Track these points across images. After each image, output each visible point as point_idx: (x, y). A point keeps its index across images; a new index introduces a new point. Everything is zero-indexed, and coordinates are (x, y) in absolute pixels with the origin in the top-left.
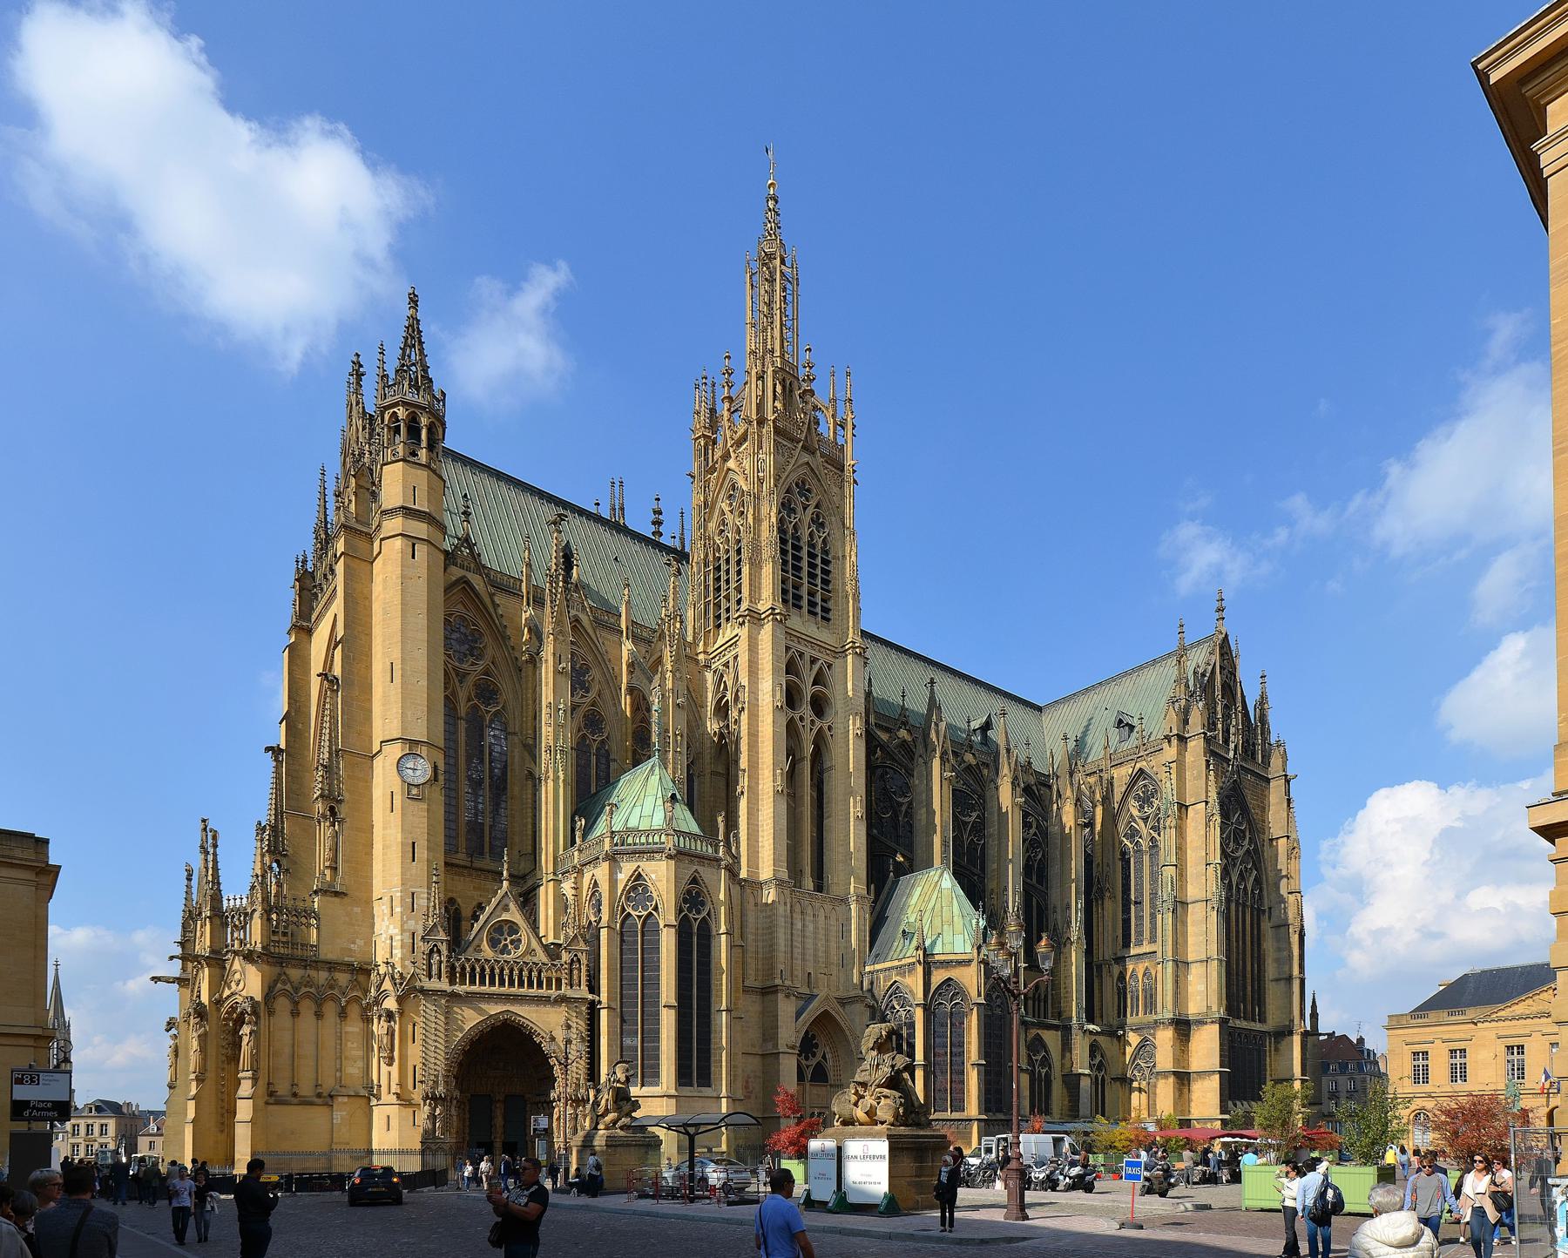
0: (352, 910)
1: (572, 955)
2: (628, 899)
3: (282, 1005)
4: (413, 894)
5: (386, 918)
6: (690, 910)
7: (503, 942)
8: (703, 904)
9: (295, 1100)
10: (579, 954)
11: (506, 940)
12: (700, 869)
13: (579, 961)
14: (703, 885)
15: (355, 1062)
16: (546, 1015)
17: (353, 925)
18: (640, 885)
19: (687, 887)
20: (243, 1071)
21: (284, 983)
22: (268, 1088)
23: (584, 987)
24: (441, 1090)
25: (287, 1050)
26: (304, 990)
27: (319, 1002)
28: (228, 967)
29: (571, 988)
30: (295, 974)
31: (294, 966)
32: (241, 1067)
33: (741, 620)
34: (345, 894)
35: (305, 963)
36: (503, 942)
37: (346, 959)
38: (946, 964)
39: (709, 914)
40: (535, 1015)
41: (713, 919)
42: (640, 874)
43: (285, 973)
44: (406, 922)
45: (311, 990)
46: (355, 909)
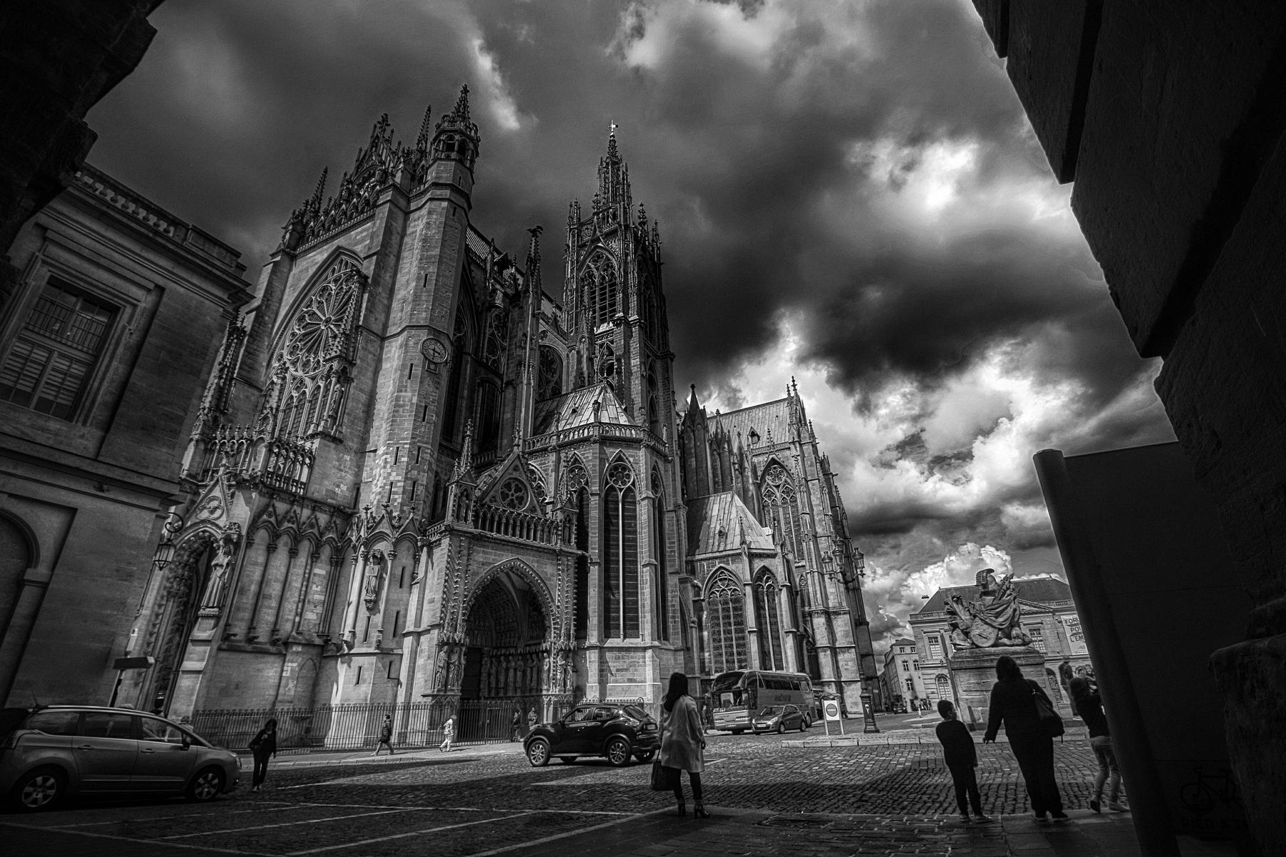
0: (343, 457)
2: (611, 475)
4: (419, 448)
5: (388, 466)
7: (510, 497)
9: (249, 648)
11: (512, 495)
15: (315, 607)
17: (341, 470)
18: (620, 465)
20: (207, 607)
22: (249, 633)
24: (459, 635)
25: (253, 588)
27: (296, 539)
28: (203, 492)
30: (281, 507)
31: (282, 500)
32: (204, 602)
34: (341, 441)
35: (294, 499)
36: (510, 497)
37: (329, 500)
38: (760, 556)
40: (536, 565)
43: (273, 505)
44: (410, 471)
46: (346, 456)
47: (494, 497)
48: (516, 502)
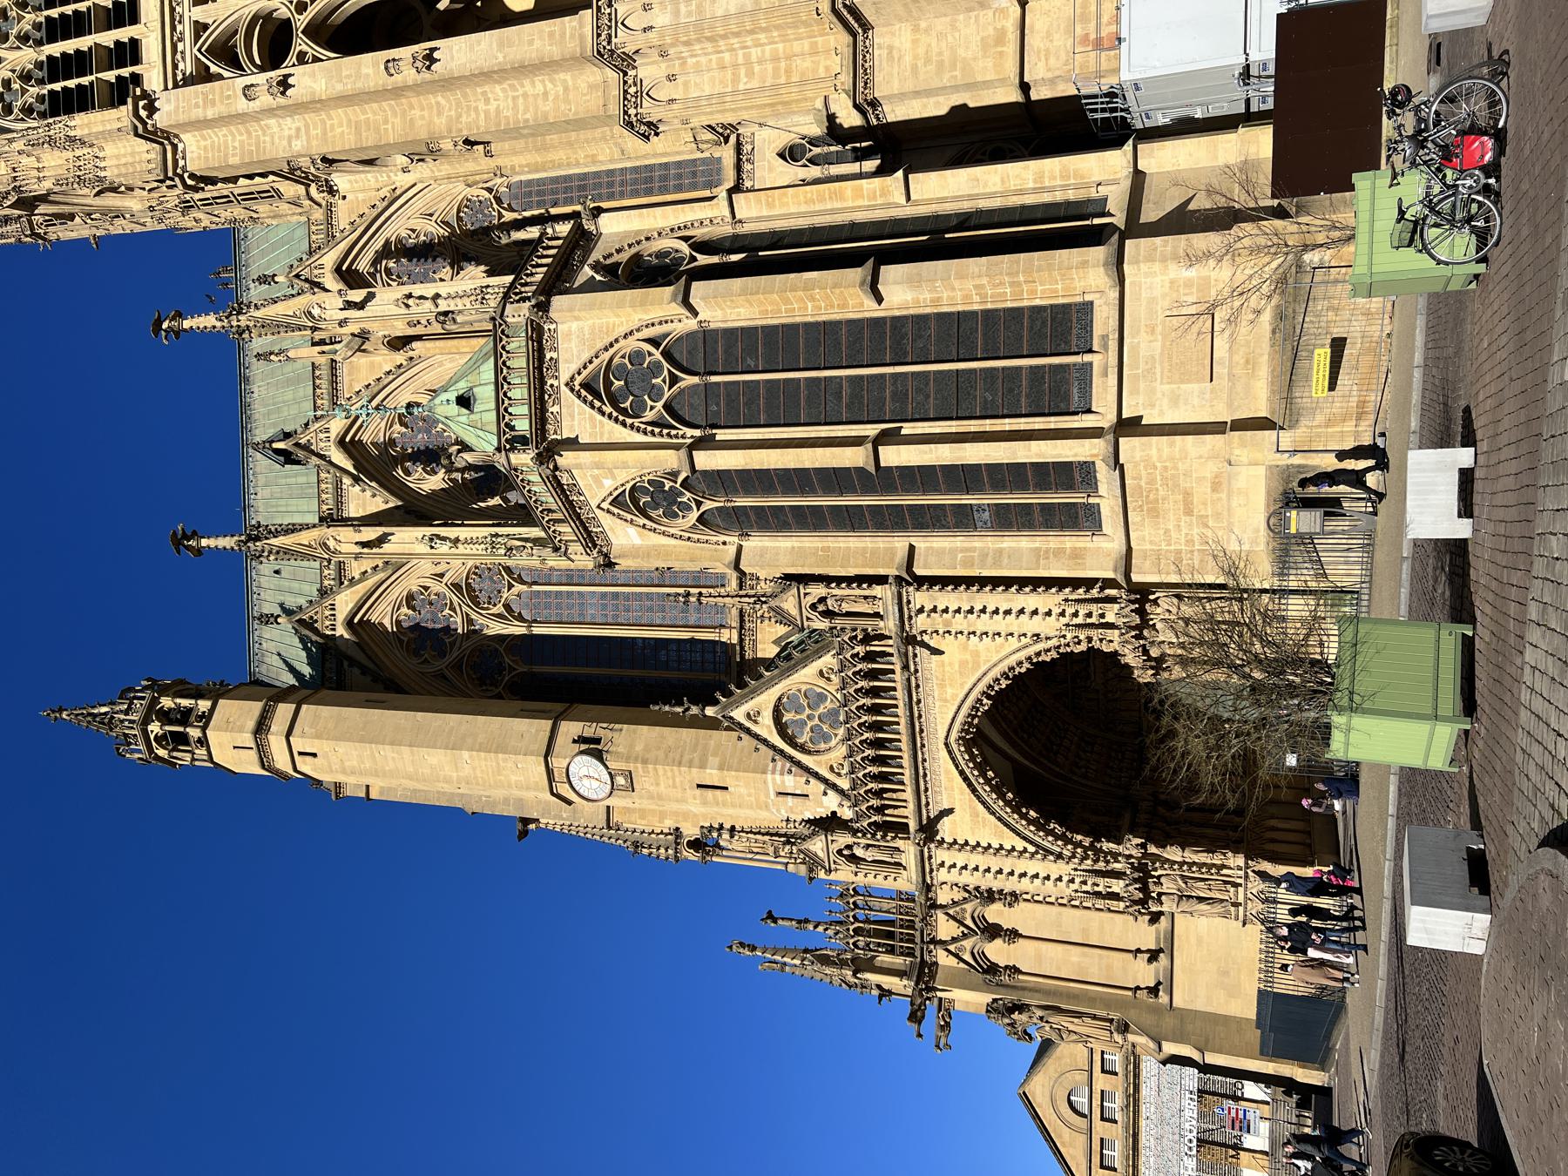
1: (814, 615)
3: (997, 951)
6: (656, 394)
8: (636, 357)
10: (810, 600)
11: (810, 717)
12: (564, 376)
13: (822, 600)
14: (596, 362)
16: (947, 668)
19: (608, 409)
21: (962, 949)
23: (877, 590)
26: (969, 922)
29: (881, 617)
33: (190, 182)
39: (654, 342)
40: (949, 691)
41: (665, 328)
42: (614, 502)
45: (969, 911)
47: (832, 768)
48: (821, 710)
